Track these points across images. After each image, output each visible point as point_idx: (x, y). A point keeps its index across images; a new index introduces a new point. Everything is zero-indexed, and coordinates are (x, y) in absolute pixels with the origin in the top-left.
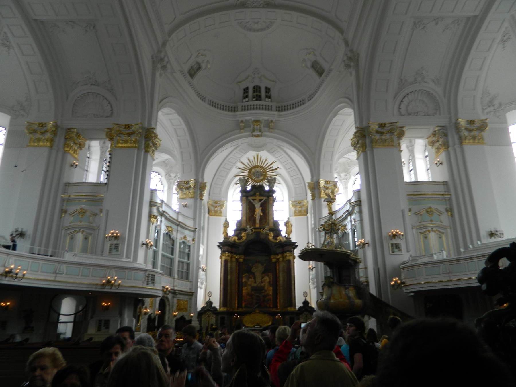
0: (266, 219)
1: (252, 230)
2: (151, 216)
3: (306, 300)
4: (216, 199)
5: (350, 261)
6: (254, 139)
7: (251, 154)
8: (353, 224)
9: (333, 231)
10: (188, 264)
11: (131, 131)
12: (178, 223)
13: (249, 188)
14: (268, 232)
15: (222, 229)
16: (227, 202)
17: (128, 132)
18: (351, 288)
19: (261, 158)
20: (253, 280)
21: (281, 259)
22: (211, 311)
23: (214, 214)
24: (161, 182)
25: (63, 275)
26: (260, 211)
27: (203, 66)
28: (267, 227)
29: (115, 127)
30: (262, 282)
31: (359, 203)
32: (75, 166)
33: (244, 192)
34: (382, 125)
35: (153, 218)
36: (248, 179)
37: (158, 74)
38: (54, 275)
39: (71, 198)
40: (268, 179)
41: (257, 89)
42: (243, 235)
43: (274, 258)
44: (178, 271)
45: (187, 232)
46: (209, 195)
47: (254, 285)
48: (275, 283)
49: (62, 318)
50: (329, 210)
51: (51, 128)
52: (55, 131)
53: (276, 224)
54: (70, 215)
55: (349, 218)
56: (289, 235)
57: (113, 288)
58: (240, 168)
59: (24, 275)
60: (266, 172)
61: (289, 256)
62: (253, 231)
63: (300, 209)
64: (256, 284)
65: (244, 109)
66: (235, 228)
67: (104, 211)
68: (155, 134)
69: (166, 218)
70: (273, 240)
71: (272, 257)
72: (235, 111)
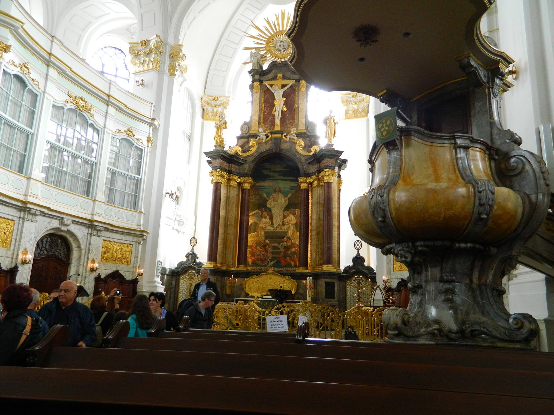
0: (293, 118)
1: (267, 137)
3: (358, 254)
4: (216, 94)
10: (138, 183)
13: (265, 67)
14: (295, 138)
20: (268, 220)
21: (315, 184)
22: (194, 269)
23: (211, 118)
24: (126, 65)
26: (283, 103)
28: (294, 130)
30: (283, 225)
46: (205, 88)
48: (303, 227)
53: (309, 126)
58: (253, 37)
61: (328, 175)
62: (270, 137)
63: (355, 107)
64: (273, 227)
70: (304, 153)
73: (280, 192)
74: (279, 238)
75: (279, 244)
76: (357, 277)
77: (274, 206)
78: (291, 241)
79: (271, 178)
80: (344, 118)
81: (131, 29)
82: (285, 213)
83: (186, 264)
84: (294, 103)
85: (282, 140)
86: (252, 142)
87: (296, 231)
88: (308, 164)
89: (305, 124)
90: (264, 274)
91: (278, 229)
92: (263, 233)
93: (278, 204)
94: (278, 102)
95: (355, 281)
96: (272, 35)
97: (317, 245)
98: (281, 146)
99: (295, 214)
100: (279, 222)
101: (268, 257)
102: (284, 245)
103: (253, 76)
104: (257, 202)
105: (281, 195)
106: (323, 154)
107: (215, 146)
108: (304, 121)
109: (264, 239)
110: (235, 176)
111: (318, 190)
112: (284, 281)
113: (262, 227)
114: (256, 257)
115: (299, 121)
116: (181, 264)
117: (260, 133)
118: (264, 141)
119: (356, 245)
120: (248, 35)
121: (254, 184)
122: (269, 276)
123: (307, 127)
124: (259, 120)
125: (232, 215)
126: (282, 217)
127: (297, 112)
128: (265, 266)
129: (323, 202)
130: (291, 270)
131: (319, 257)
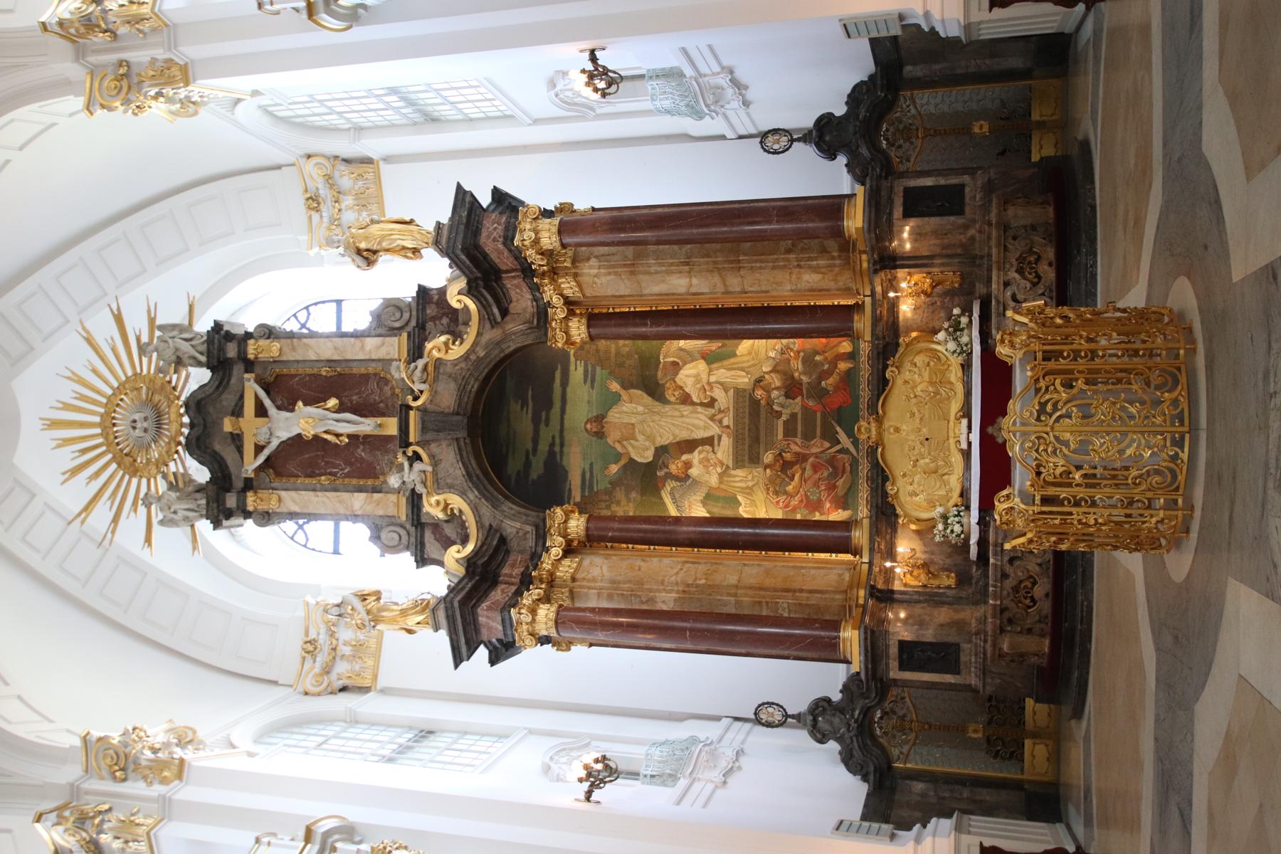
0: (365, 378)
3: (806, 137)
13: (201, 474)
14: (420, 363)
19: (67, 407)
20: (695, 457)
21: (569, 287)
22: (867, 712)
26: (310, 409)
28: (399, 372)
30: (712, 403)
36: (165, 476)
47: (725, 449)
58: (116, 520)
64: (720, 437)
73: (603, 417)
74: (758, 415)
75: (779, 414)
76: (887, 140)
77: (650, 438)
78: (767, 376)
79: (557, 449)
82: (672, 399)
83: (848, 741)
84: (316, 377)
85: (429, 406)
86: (432, 508)
87: (732, 360)
88: (508, 318)
89: (381, 338)
90: (882, 454)
91: (725, 422)
92: (740, 473)
93: (643, 422)
94: (307, 422)
95: (900, 147)
96: (113, 459)
97: (774, 268)
98: (447, 411)
99: (675, 364)
100: (703, 417)
101: (822, 452)
102: (782, 399)
103: (229, 514)
104: (633, 495)
105: (614, 416)
106: (463, 250)
107: (436, 629)
109: (761, 470)
110: (542, 563)
111: (589, 275)
112: (906, 382)
113: (721, 475)
114: (824, 495)
115: (373, 357)
116: (848, 760)
119: (776, 147)
120: (109, 535)
121: (575, 504)
122: (889, 437)
123: (394, 331)
124: (366, 492)
125: (675, 571)
126: (686, 409)
127: (344, 365)
128: (855, 463)
129: (630, 251)
130: (865, 371)
131: (816, 259)
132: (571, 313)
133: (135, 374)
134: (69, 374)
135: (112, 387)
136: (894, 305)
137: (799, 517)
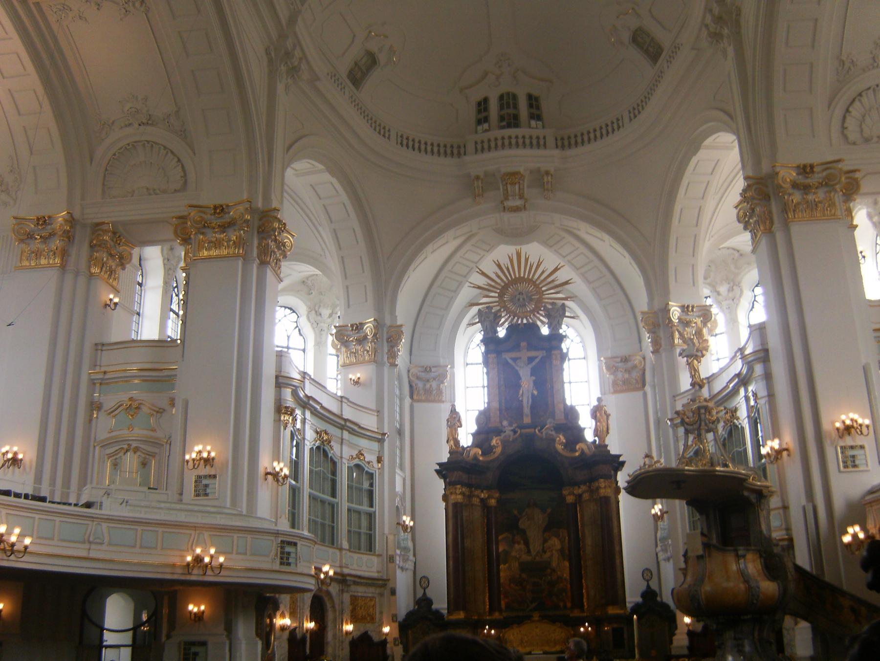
1: (515, 432)
2: (280, 409)
3: (648, 586)
5: (746, 493)
6: (508, 217)
7: (503, 252)
8: (752, 406)
9: (703, 424)
10: (371, 516)
11: (227, 218)
12: (343, 423)
13: (502, 332)
14: (553, 433)
15: (444, 431)
16: (453, 367)
17: (219, 222)
18: (750, 556)
19: (527, 260)
20: (522, 546)
21: (586, 496)
24: (299, 330)
25: (104, 547)
26: (532, 385)
27: (382, 58)
28: (550, 423)
29: (194, 213)
30: (544, 552)
31: (763, 355)
32: (112, 306)
33: (490, 341)
34: (806, 170)
35: (286, 413)
36: (499, 311)
37: (280, 88)
38: (86, 546)
39: (107, 377)
40: (546, 309)
41: (508, 101)
42: (494, 442)
43: (569, 494)
44: (349, 531)
45: (363, 443)
46: (411, 355)
47: (525, 558)
48: (574, 555)
49: (109, 638)
50: (692, 376)
51: (61, 225)
52: (69, 231)
53: (571, 414)
54: (109, 414)
55: (742, 392)
56: (602, 439)
57: (209, 572)
58: (479, 288)
59: (26, 547)
60: (542, 293)
61: (605, 487)
62: (518, 434)
65: (482, 147)
66: (473, 428)
67: (179, 403)
68: (280, 221)
69: (315, 413)
71: (565, 492)
72: (459, 155)
80: (612, 390)
81: (309, 282)
92: (517, 565)
108: (562, 406)
117: (505, 427)
118: (511, 440)
119: (645, 575)
132: (576, 495)
133: (543, 291)
134: (541, 261)
135: (537, 280)
136: (584, 626)
137: (502, 589)
